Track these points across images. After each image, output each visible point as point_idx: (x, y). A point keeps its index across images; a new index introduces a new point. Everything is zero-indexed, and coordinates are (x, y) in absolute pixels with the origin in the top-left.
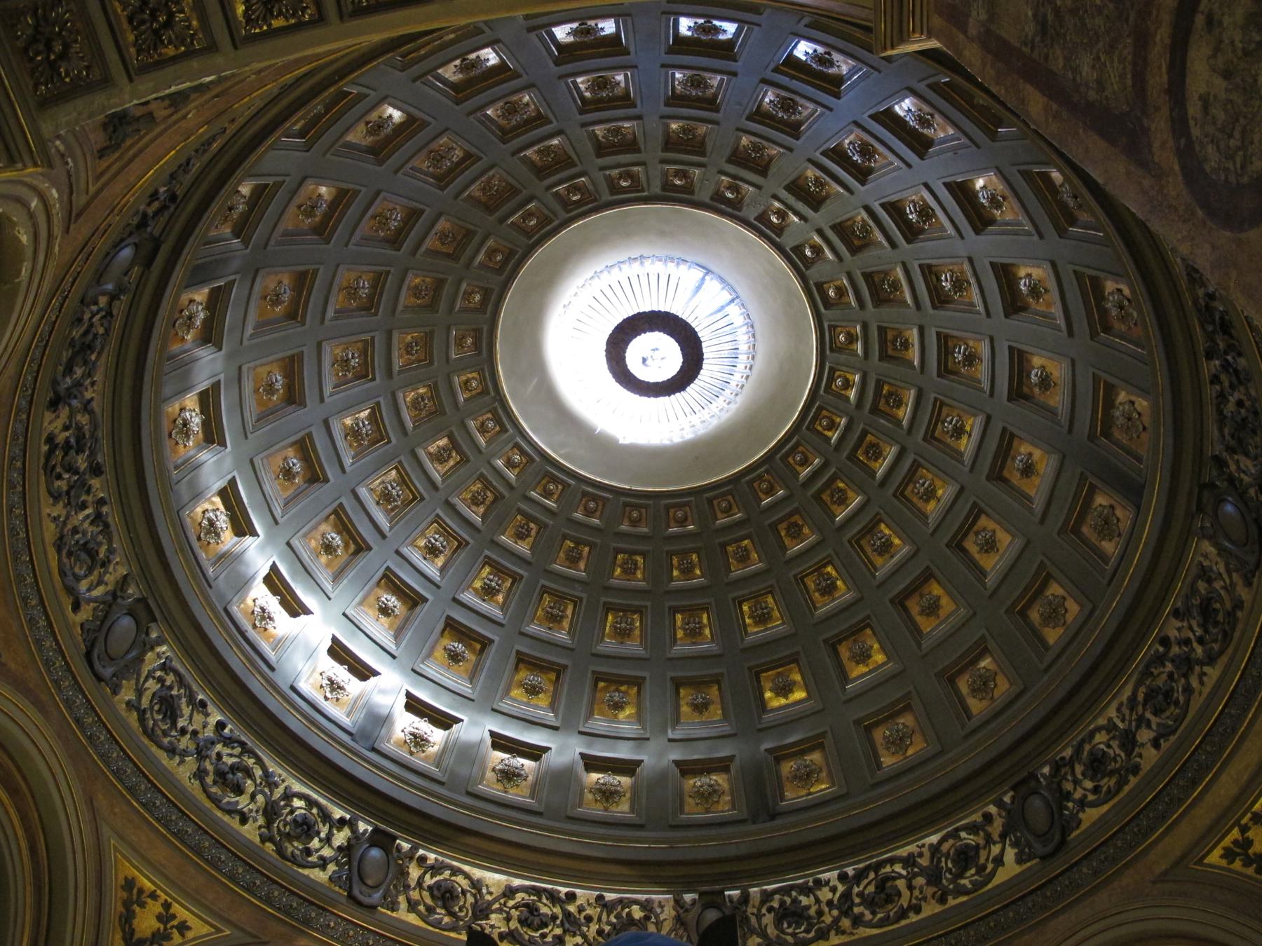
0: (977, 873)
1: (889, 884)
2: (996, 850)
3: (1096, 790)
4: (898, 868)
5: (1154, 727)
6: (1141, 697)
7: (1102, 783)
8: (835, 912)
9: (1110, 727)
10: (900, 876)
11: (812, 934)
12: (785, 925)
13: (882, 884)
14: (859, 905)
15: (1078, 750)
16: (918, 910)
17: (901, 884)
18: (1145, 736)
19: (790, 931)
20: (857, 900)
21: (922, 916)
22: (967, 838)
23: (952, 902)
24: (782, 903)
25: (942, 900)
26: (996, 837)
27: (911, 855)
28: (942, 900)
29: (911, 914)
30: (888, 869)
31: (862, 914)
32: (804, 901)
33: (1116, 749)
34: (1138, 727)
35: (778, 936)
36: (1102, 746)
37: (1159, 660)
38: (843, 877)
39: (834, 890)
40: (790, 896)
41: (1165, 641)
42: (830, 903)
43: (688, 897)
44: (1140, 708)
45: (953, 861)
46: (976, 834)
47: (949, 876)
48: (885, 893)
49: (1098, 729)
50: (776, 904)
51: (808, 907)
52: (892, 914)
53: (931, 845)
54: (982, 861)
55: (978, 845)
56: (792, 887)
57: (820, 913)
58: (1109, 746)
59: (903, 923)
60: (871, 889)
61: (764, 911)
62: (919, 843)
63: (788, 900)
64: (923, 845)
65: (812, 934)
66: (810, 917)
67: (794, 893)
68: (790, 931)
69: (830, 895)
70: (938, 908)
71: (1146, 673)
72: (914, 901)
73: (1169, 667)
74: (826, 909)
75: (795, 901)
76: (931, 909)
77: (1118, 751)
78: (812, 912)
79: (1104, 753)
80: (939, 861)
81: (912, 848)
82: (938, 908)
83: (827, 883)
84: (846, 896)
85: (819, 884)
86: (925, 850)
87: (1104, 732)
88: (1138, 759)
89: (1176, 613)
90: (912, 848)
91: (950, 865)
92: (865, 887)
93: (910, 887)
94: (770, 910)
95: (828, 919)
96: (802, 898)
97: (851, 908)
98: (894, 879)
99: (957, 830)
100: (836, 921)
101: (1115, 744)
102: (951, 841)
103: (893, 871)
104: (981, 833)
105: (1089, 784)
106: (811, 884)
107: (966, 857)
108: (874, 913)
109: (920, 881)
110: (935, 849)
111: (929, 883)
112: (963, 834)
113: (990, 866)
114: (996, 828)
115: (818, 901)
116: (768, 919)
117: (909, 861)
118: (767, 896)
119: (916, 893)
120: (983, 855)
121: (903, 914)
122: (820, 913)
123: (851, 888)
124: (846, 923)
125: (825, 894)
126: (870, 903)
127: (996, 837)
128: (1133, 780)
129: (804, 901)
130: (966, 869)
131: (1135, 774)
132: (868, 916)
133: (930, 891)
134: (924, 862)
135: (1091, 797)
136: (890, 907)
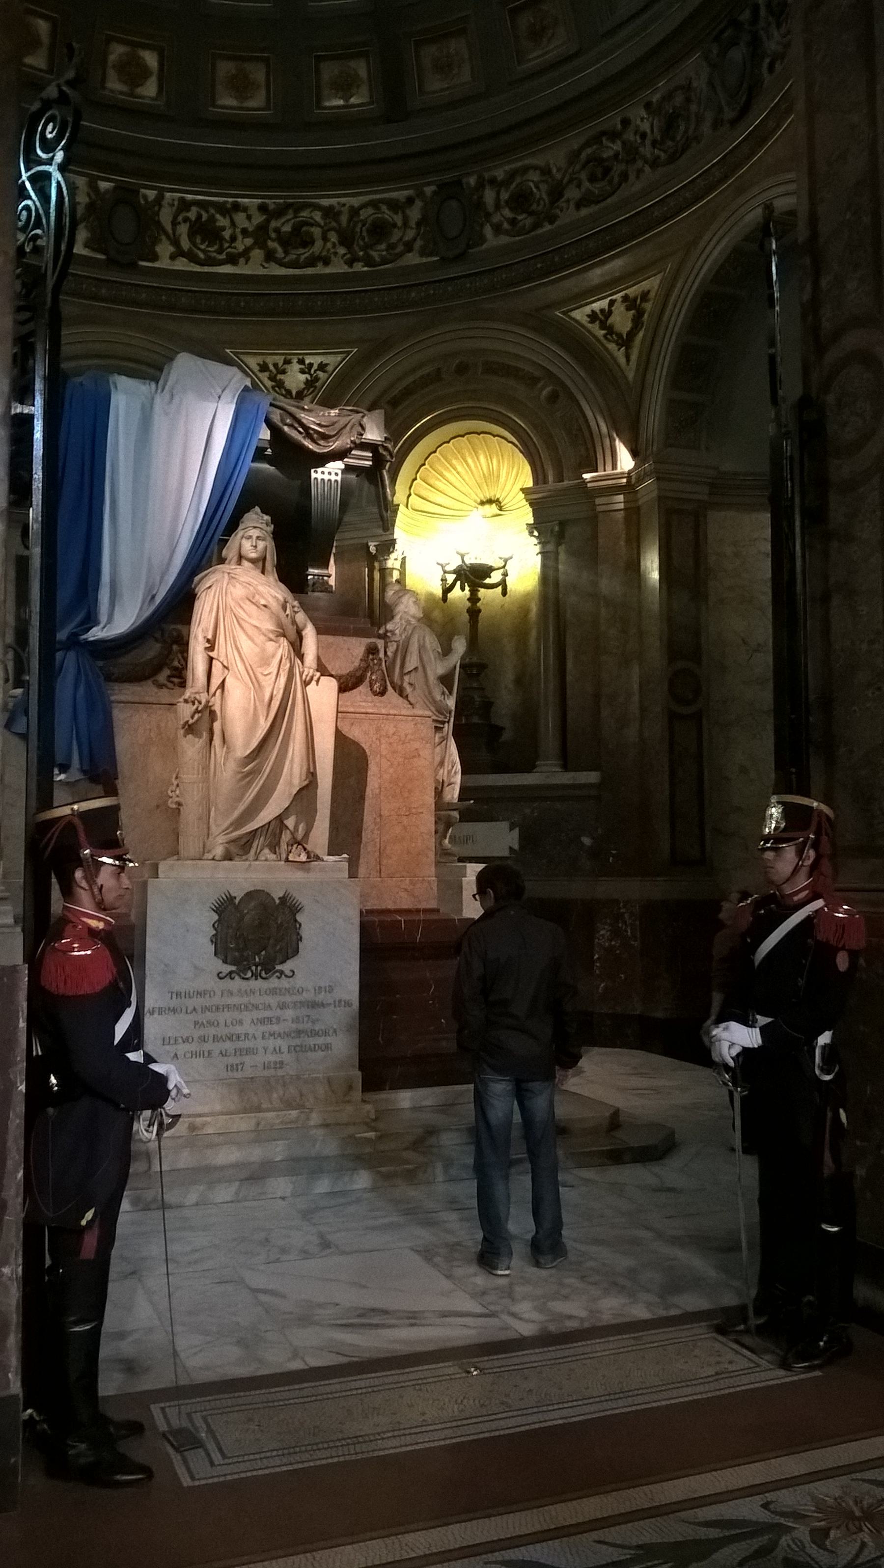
0: (387, 250)
1: (304, 229)
2: (410, 234)
3: (513, 222)
4: (317, 216)
5: (583, 190)
6: (583, 156)
7: (520, 218)
8: (249, 241)
9: (546, 171)
10: (318, 225)
11: (223, 256)
12: (198, 240)
13: (297, 229)
14: (273, 240)
15: (512, 175)
16: (327, 262)
17: (316, 231)
18: (572, 193)
19: (203, 247)
20: (273, 235)
21: (328, 270)
22: (387, 214)
23: (359, 267)
24: (199, 216)
25: (350, 263)
26: (413, 223)
27: (331, 208)
28: (350, 263)
29: (320, 264)
30: (305, 214)
31: (274, 251)
32: (222, 221)
33: (542, 193)
34: (571, 181)
35: (190, 249)
36: (532, 184)
37: (614, 136)
38: (262, 208)
39: (249, 218)
40: (207, 212)
41: (626, 122)
42: (244, 232)
43: (104, 185)
44: (578, 167)
45: (368, 231)
46: (396, 213)
47: (362, 243)
48: (298, 238)
49: (535, 168)
50: (192, 214)
51: (223, 229)
52: (303, 257)
53: (352, 208)
54: (394, 239)
55: (395, 225)
56: (212, 203)
57: (233, 239)
58: (537, 187)
59: (309, 271)
60: (287, 228)
61: (180, 218)
62: (343, 200)
63: (205, 216)
64: (344, 205)
65: (223, 256)
66: (222, 239)
67: (212, 211)
68: (203, 247)
69: (246, 224)
70: (345, 269)
71: (596, 140)
72: (324, 253)
73: (617, 146)
74: (240, 237)
75: (212, 219)
76: (338, 267)
77: (545, 196)
78: (227, 234)
79: (532, 192)
80: (355, 226)
81: (333, 201)
82: (345, 269)
83: (245, 209)
84: (263, 228)
85: (236, 207)
86: (345, 210)
87: (538, 172)
88: (558, 211)
89: (648, 106)
90: (333, 201)
91: (365, 234)
92: (283, 224)
93: (325, 239)
94: (187, 219)
95: (240, 245)
96: (218, 216)
97: (265, 241)
98: (312, 225)
99: (381, 201)
100: (247, 250)
101: (544, 187)
102: (370, 210)
103: (311, 218)
104: (400, 212)
105: (507, 213)
106: (229, 206)
107: (380, 230)
108: (286, 253)
109: (333, 237)
110: (354, 212)
111: (342, 243)
112: (384, 208)
113: (400, 248)
114: (415, 214)
115: (233, 224)
116: (183, 230)
117: (329, 213)
118: (185, 205)
119: (329, 245)
120: (396, 235)
121: (312, 262)
122: (233, 239)
123: (268, 221)
124: (257, 254)
125: (240, 218)
126: (286, 242)
127: (413, 223)
128: (547, 227)
129: (222, 221)
130: (379, 242)
131: (551, 222)
132: (280, 253)
133: (342, 251)
134: (344, 219)
135: (506, 226)
136: (301, 251)
